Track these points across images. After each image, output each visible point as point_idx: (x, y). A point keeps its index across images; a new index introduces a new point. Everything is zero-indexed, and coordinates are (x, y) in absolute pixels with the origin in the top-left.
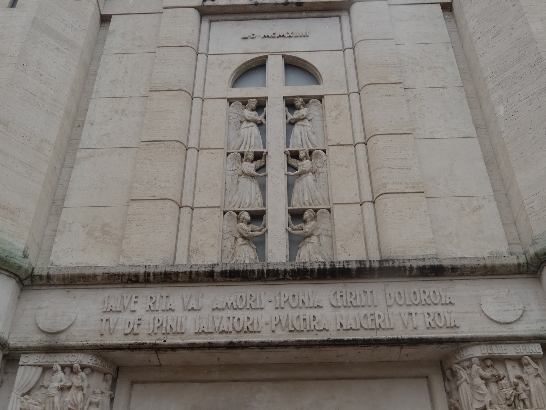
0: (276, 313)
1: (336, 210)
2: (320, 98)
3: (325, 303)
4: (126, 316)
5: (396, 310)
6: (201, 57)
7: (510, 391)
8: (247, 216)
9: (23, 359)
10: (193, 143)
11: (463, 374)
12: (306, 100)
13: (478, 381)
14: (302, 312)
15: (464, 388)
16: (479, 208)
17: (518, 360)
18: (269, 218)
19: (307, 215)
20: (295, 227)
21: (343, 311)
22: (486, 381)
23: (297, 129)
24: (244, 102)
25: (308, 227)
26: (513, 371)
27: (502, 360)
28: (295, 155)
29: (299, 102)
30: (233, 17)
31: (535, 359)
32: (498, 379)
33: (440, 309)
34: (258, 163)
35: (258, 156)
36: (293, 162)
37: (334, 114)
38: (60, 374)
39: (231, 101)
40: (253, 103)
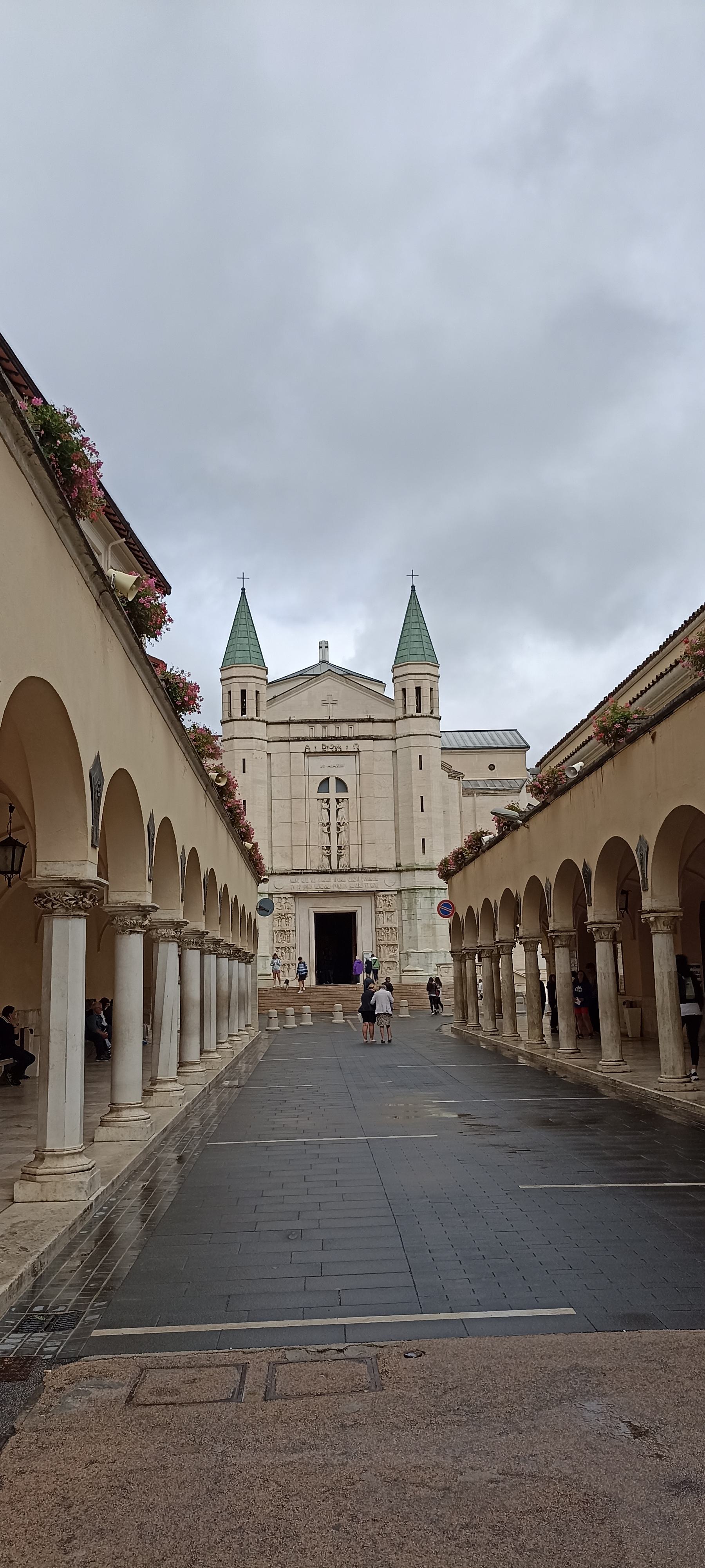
0: (335, 883)
1: (351, 846)
2: (347, 799)
3: (347, 880)
4: (297, 884)
5: (364, 882)
6: (307, 777)
7: (388, 903)
8: (325, 848)
9: (274, 896)
10: (308, 821)
11: (378, 898)
12: (343, 799)
13: (381, 901)
14: (341, 883)
15: (378, 902)
16: (390, 848)
17: (392, 895)
18: (332, 848)
19: (342, 848)
20: (339, 851)
21: (351, 883)
22: (383, 900)
23: (339, 812)
24: (323, 800)
25: (343, 851)
26: (390, 898)
27: (388, 895)
28: (339, 823)
29: (340, 800)
30: (316, 754)
31: (395, 895)
32: (386, 900)
33: (375, 882)
34: (328, 826)
35: (328, 824)
36: (339, 826)
37: (352, 807)
38: (283, 900)
39: (318, 799)
40: (325, 800)
